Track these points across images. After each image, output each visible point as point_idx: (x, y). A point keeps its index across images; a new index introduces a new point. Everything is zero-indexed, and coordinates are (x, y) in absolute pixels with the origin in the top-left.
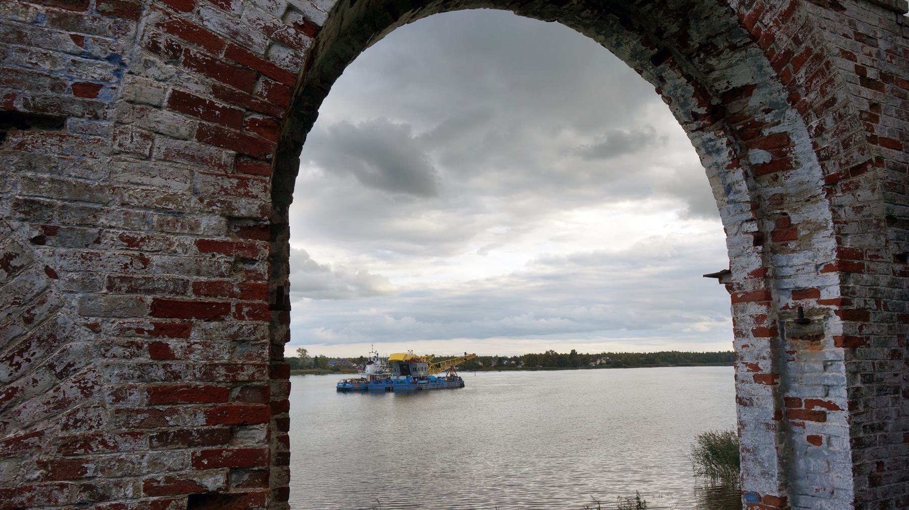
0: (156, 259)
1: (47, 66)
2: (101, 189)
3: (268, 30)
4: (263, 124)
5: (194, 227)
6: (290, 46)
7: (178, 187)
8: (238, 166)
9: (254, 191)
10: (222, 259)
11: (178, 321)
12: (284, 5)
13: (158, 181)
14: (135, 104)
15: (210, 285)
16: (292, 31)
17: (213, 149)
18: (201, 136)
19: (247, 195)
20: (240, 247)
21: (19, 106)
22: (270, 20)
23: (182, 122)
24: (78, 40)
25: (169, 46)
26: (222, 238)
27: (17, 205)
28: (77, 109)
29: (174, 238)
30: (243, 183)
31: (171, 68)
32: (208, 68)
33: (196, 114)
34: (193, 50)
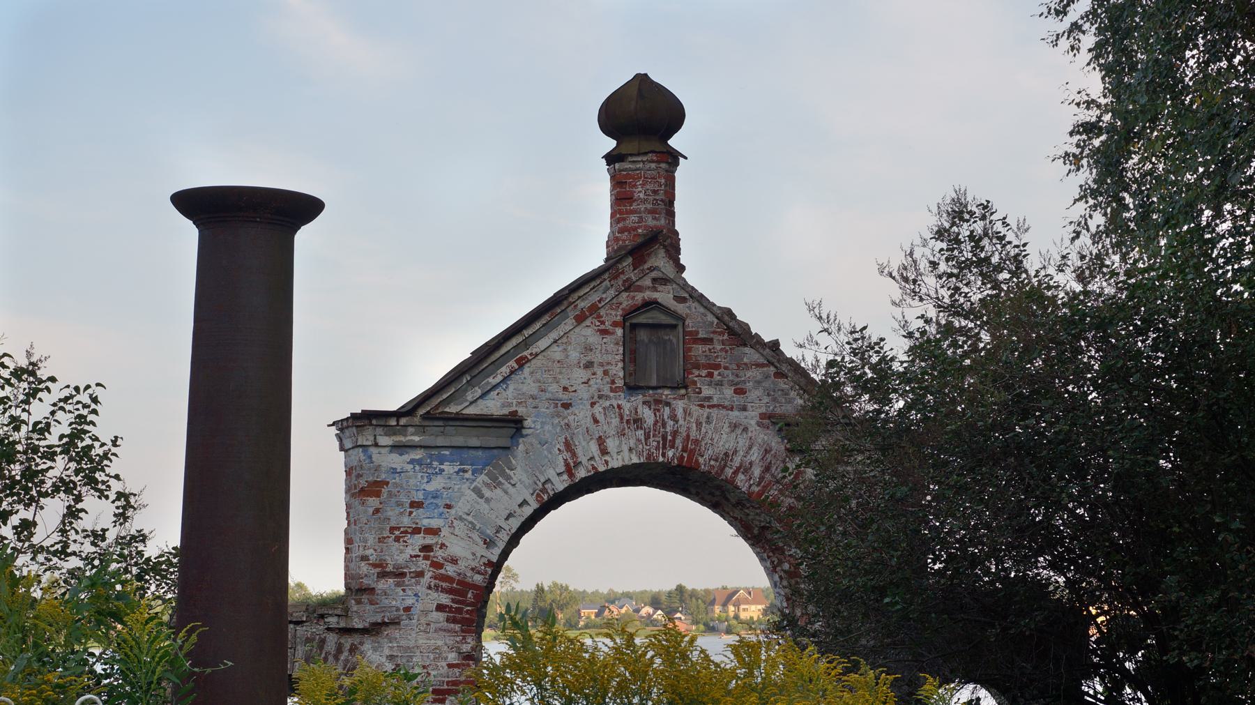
0: (433, 673)
1: (394, 603)
2: (413, 648)
3: (473, 569)
4: (472, 611)
5: (446, 658)
6: (482, 574)
7: (440, 643)
8: (463, 631)
9: (469, 641)
10: (456, 670)
11: (441, 697)
12: (479, 556)
13: (433, 641)
14: (425, 612)
15: (452, 681)
16: (483, 568)
17: (452, 625)
18: (448, 621)
19: (466, 643)
20: (463, 665)
21: (386, 620)
22: (473, 564)
23: (441, 616)
24: (404, 590)
25: (435, 586)
26: (457, 662)
27: (387, 657)
28: (404, 617)
29: (439, 664)
30: (464, 638)
31: (436, 595)
32: (449, 591)
33: (446, 612)
34: (444, 585)
